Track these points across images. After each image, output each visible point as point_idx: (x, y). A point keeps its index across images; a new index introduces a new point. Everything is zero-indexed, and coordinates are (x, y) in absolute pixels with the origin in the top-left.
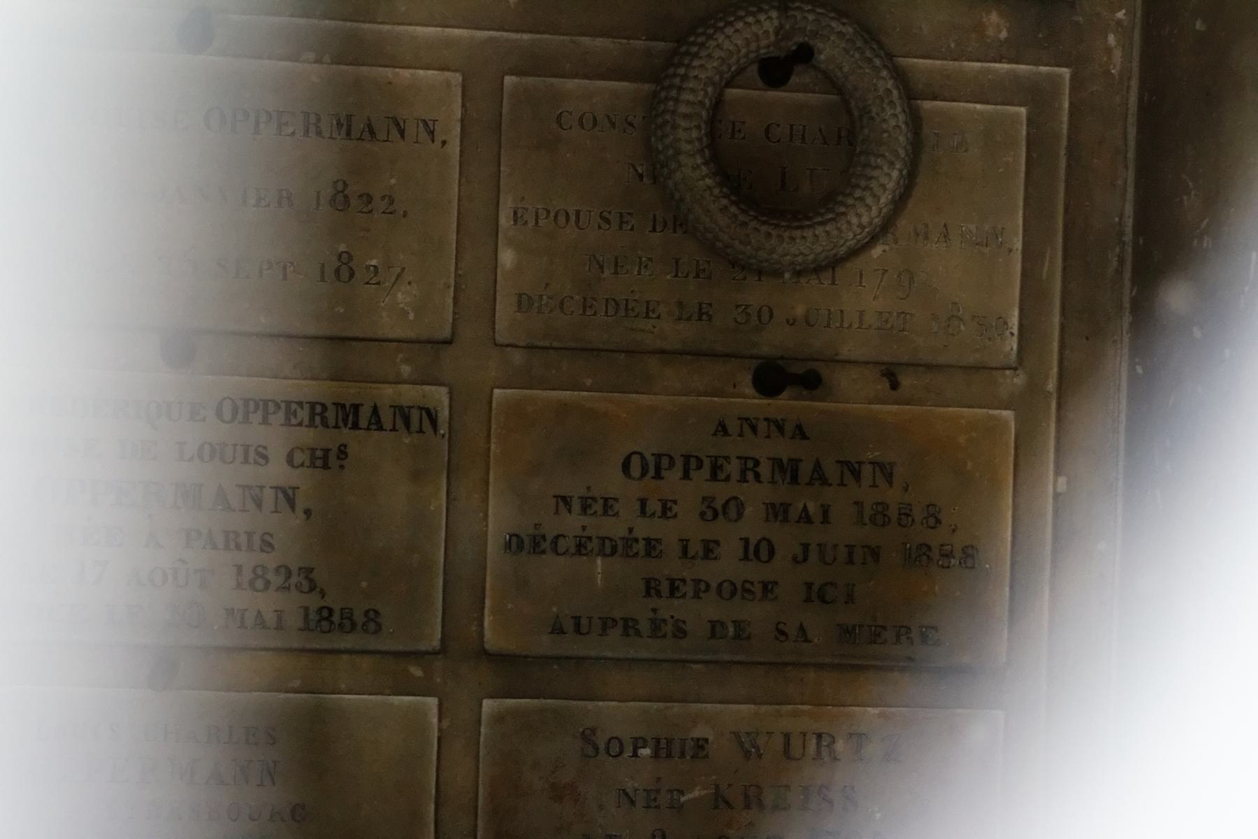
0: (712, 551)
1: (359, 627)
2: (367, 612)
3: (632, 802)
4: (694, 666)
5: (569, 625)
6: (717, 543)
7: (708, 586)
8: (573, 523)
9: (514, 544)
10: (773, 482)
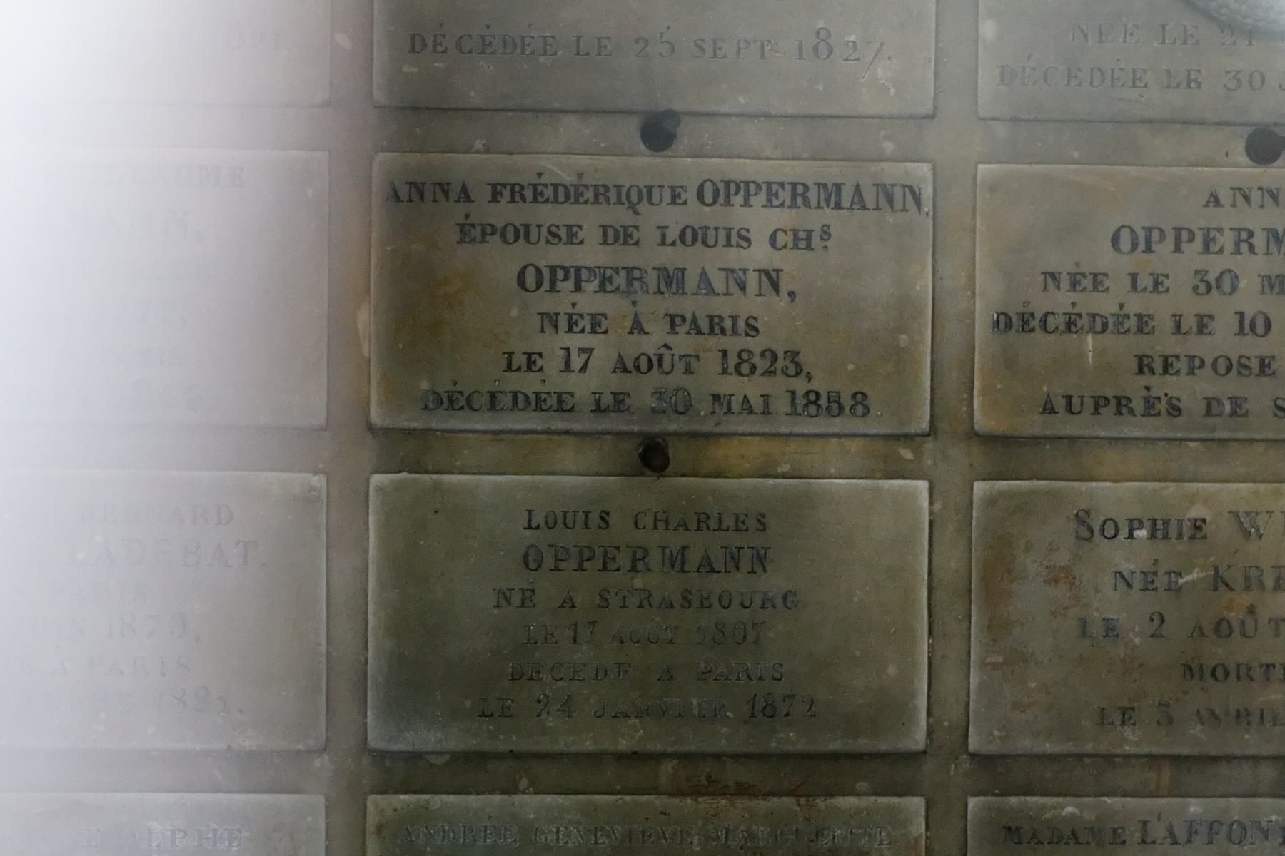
0: (1206, 326)
2: (855, 394)
3: (1129, 585)
4: (1191, 444)
5: (1060, 404)
6: (1211, 317)
7: (1202, 361)
9: (1002, 323)
10: (1268, 253)
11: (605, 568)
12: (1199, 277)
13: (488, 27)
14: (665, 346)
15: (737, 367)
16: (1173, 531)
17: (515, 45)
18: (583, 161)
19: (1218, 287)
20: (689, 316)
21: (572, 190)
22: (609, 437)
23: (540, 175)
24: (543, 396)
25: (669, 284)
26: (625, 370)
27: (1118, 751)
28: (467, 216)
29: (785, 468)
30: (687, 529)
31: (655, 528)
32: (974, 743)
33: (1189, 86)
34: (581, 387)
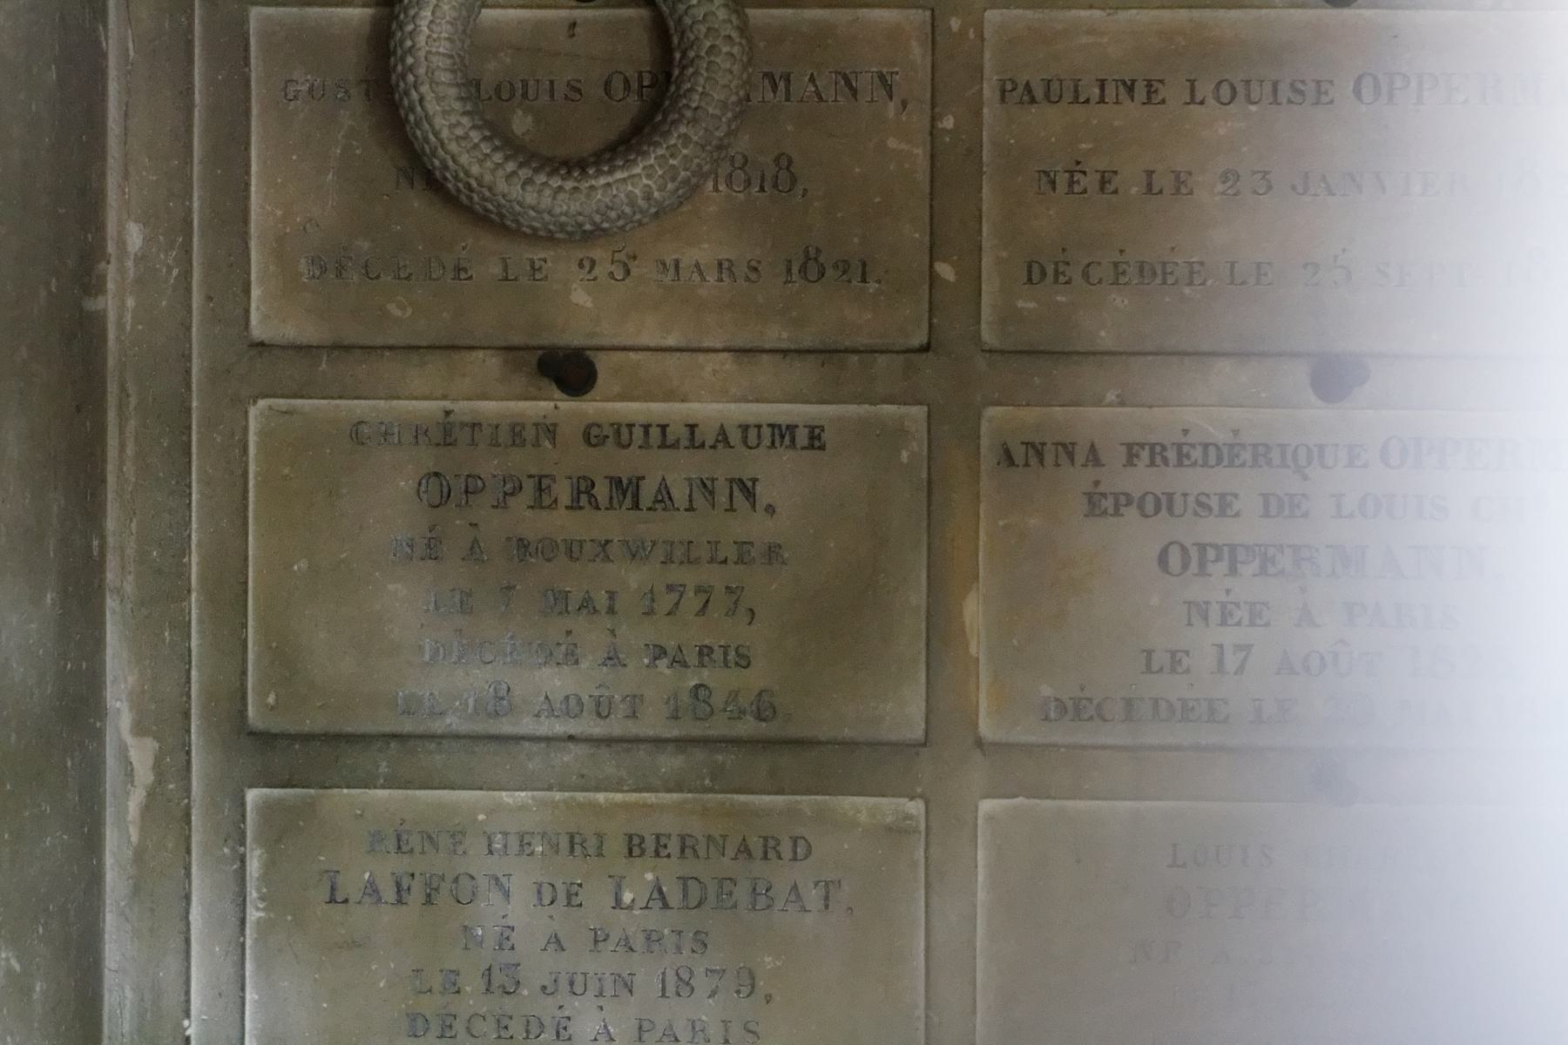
17: (1155, 274)
21: (1225, 450)
23: (1186, 432)
28: (1097, 483)
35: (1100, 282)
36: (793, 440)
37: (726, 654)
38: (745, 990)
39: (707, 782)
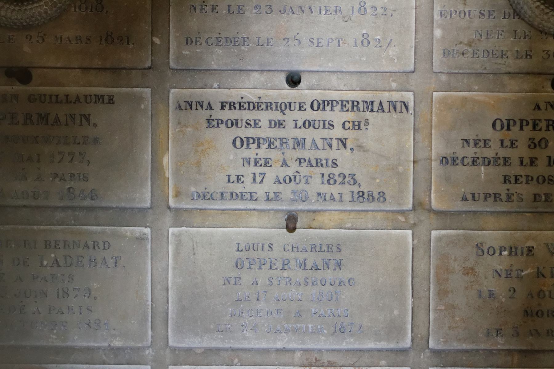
0: (534, 162)
1: (376, 200)
2: (380, 193)
3: (500, 275)
4: (527, 214)
5: (469, 197)
6: (536, 159)
8: (470, 152)
11: (271, 268)
12: (531, 141)
13: (219, 34)
14: (297, 172)
15: (328, 181)
16: (519, 252)
17: (231, 42)
18: (260, 92)
19: (539, 145)
20: (307, 159)
21: (256, 104)
22: (272, 212)
23: (242, 98)
24: (244, 194)
25: (298, 144)
26: (280, 183)
27: (495, 348)
28: (211, 116)
29: (349, 225)
30: (306, 251)
31: (293, 251)
32: (432, 344)
33: (526, 57)
34: (260, 190)
35: (212, 44)
36: (103, 101)
37: (79, 176)
38: (87, 296)
39: (73, 222)
